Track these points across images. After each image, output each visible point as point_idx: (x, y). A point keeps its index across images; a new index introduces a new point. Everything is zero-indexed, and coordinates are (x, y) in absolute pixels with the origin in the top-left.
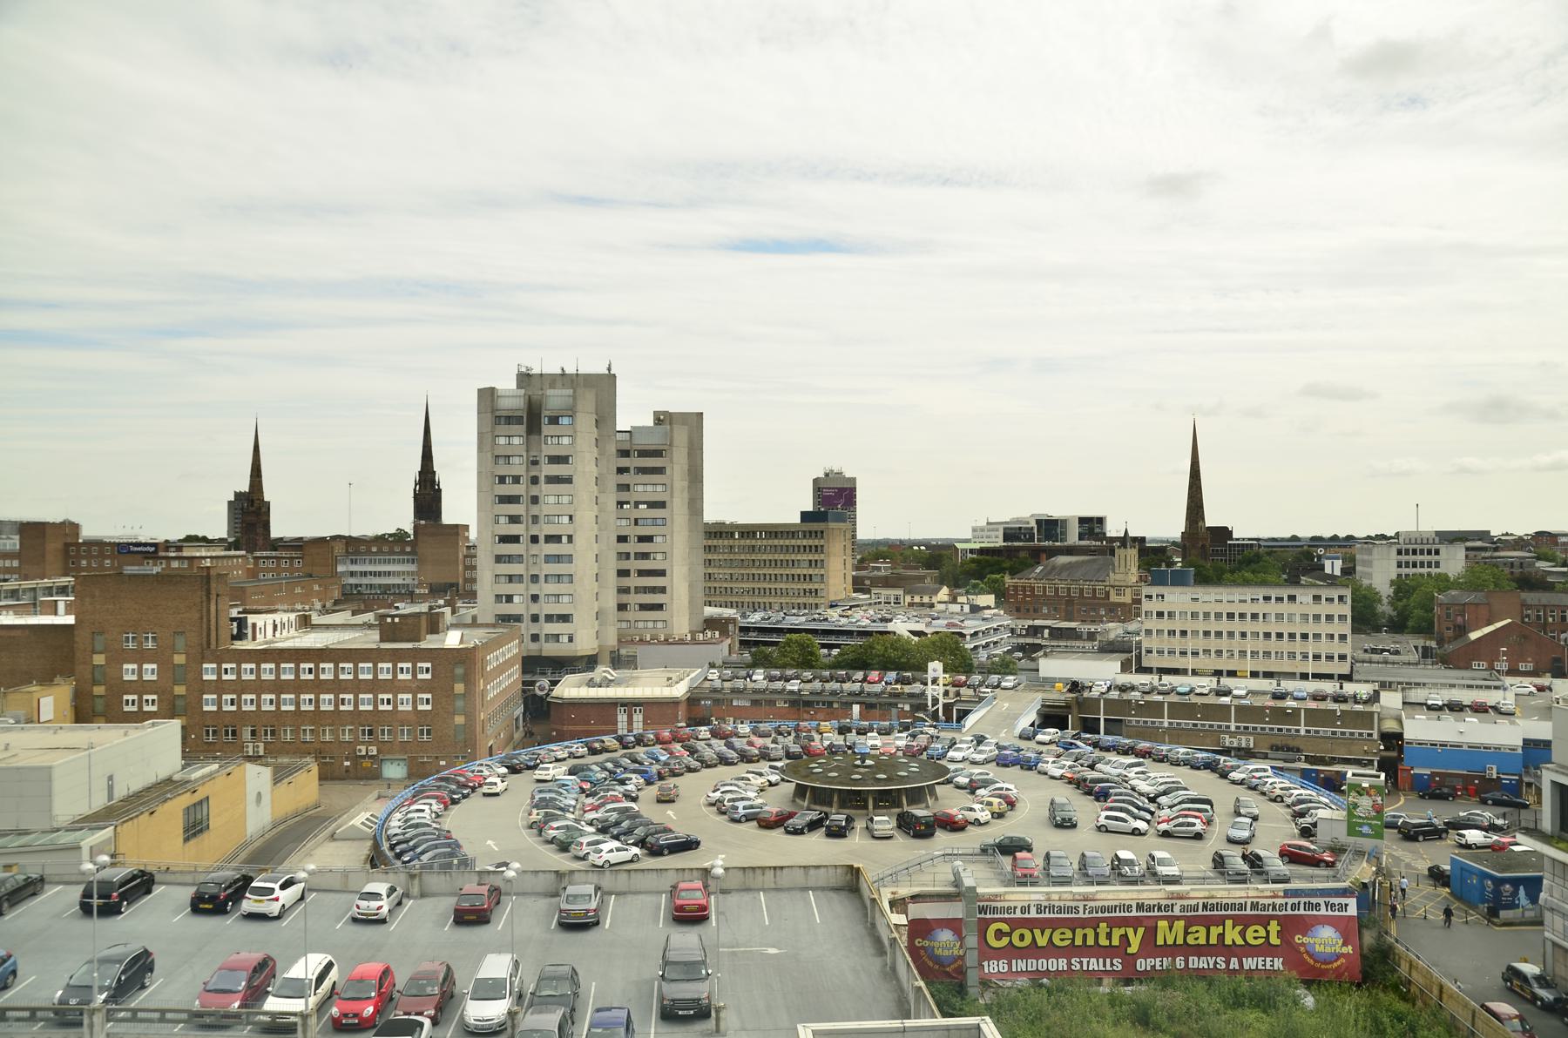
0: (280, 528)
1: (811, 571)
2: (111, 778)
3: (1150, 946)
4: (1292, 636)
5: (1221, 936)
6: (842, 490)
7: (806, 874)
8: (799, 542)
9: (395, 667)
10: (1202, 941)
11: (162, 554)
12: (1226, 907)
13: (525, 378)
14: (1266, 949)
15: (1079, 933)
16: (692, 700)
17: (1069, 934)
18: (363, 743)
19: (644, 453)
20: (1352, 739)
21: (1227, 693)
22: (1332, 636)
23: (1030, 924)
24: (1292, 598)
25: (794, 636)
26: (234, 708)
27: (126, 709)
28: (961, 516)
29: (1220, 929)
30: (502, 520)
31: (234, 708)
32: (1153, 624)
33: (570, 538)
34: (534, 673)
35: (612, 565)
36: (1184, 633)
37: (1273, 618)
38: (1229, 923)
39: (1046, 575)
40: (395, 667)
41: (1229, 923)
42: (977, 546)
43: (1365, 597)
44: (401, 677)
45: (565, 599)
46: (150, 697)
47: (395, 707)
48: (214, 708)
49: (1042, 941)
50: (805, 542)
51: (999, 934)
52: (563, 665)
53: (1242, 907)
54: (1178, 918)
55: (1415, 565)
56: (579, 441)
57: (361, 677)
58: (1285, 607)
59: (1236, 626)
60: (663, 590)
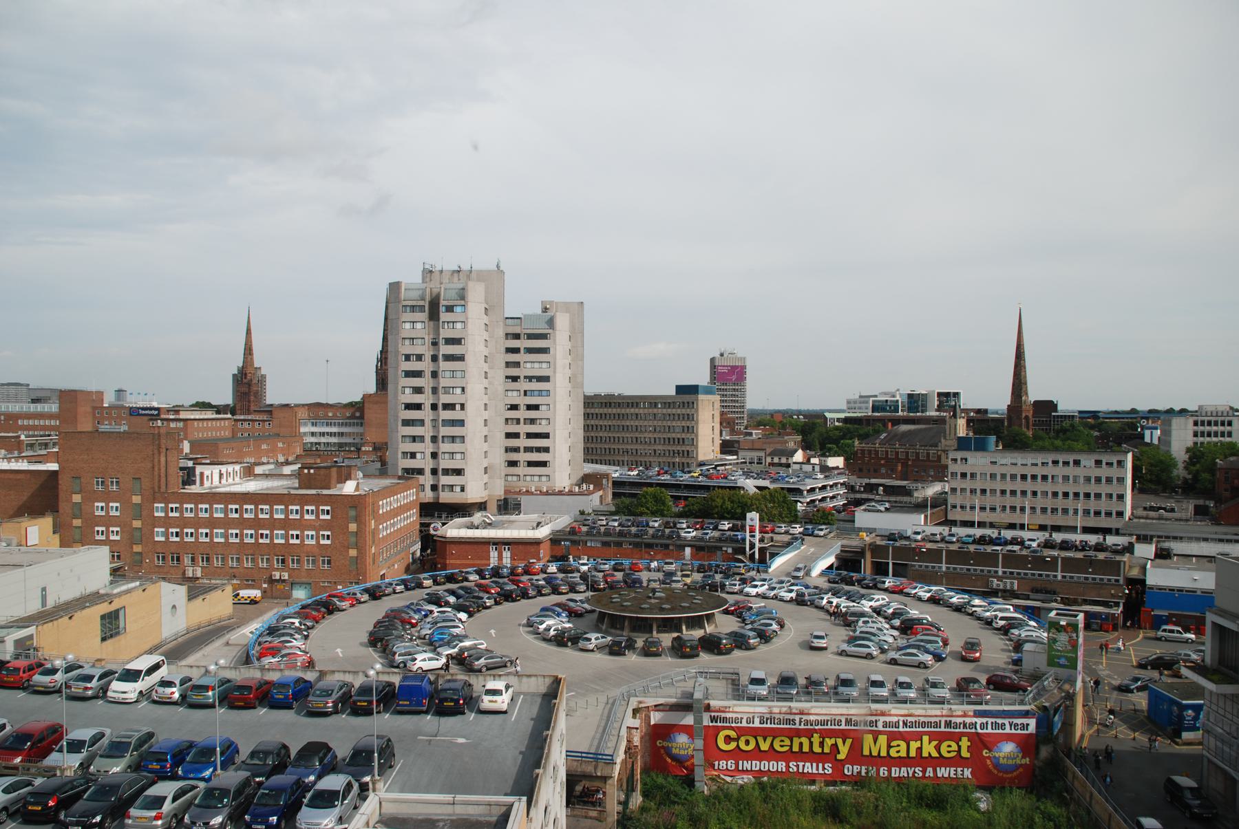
0: (273, 396)
1: (684, 436)
2: (44, 589)
3: (856, 754)
4: (1076, 495)
5: (920, 750)
6: (734, 368)
7: (520, 682)
8: (597, 411)
9: (302, 508)
10: (903, 754)
11: (163, 416)
12: (924, 724)
13: (428, 273)
14: (957, 761)
15: (796, 741)
16: (555, 540)
17: (787, 742)
18: (277, 569)
19: (531, 337)
20: (1101, 585)
21: (1022, 543)
22: (1110, 496)
23: (755, 733)
24: (1077, 463)
25: (650, 490)
26: (207, 540)
27: (97, 538)
28: (833, 394)
29: (918, 744)
30: (408, 391)
31: (207, 540)
32: (958, 483)
33: (463, 406)
34: (432, 516)
35: (500, 429)
36: (983, 491)
37: (1060, 480)
38: (926, 738)
39: (887, 441)
40: (302, 508)
41: (926, 738)
42: (842, 416)
43: (1161, 462)
44: (307, 517)
45: (458, 456)
46: (115, 529)
47: (303, 541)
48: (163, 539)
49: (765, 746)
50: (601, 411)
51: (728, 739)
52: (461, 510)
53: (937, 725)
54: (880, 733)
55: (1209, 435)
56: (470, 326)
57: (276, 516)
58: (1071, 471)
59: (1029, 486)
60: (546, 450)
